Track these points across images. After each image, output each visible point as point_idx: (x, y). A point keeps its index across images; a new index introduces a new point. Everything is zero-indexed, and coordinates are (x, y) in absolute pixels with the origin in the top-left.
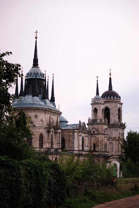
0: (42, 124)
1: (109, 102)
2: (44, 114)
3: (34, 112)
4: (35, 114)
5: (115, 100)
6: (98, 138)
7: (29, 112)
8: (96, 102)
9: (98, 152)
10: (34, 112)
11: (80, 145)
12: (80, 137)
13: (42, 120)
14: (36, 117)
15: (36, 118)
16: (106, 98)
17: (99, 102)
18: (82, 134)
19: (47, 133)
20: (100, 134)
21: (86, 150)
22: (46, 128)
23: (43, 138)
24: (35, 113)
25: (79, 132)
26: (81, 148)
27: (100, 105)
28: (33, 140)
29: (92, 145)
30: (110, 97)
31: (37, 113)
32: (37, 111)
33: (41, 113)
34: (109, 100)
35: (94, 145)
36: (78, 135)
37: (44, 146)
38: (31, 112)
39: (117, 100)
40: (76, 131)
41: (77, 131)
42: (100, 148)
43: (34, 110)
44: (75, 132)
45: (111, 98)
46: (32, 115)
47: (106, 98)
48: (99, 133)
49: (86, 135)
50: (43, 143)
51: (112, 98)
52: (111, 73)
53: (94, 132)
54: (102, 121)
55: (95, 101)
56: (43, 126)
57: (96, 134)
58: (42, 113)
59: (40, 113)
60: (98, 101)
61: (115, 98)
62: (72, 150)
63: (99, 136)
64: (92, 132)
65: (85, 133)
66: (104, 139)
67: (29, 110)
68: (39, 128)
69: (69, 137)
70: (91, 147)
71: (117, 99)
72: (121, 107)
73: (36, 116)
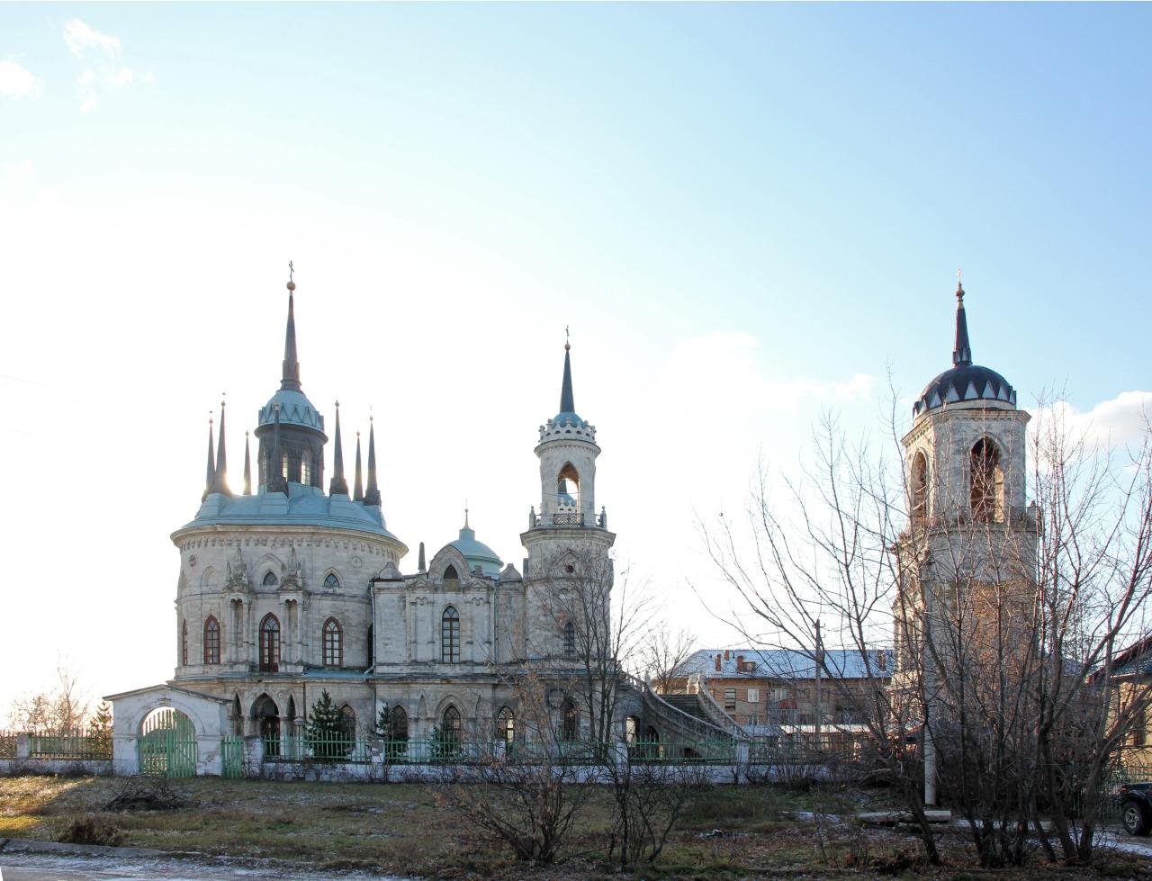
0: (216, 582)
10: (189, 548)
11: (424, 637)
15: (192, 566)
18: (430, 596)
19: (233, 612)
21: (478, 659)
23: (218, 631)
37: (223, 658)
40: (379, 589)
41: (395, 585)
49: (470, 596)
50: (219, 648)
58: (210, 544)
65: (465, 589)
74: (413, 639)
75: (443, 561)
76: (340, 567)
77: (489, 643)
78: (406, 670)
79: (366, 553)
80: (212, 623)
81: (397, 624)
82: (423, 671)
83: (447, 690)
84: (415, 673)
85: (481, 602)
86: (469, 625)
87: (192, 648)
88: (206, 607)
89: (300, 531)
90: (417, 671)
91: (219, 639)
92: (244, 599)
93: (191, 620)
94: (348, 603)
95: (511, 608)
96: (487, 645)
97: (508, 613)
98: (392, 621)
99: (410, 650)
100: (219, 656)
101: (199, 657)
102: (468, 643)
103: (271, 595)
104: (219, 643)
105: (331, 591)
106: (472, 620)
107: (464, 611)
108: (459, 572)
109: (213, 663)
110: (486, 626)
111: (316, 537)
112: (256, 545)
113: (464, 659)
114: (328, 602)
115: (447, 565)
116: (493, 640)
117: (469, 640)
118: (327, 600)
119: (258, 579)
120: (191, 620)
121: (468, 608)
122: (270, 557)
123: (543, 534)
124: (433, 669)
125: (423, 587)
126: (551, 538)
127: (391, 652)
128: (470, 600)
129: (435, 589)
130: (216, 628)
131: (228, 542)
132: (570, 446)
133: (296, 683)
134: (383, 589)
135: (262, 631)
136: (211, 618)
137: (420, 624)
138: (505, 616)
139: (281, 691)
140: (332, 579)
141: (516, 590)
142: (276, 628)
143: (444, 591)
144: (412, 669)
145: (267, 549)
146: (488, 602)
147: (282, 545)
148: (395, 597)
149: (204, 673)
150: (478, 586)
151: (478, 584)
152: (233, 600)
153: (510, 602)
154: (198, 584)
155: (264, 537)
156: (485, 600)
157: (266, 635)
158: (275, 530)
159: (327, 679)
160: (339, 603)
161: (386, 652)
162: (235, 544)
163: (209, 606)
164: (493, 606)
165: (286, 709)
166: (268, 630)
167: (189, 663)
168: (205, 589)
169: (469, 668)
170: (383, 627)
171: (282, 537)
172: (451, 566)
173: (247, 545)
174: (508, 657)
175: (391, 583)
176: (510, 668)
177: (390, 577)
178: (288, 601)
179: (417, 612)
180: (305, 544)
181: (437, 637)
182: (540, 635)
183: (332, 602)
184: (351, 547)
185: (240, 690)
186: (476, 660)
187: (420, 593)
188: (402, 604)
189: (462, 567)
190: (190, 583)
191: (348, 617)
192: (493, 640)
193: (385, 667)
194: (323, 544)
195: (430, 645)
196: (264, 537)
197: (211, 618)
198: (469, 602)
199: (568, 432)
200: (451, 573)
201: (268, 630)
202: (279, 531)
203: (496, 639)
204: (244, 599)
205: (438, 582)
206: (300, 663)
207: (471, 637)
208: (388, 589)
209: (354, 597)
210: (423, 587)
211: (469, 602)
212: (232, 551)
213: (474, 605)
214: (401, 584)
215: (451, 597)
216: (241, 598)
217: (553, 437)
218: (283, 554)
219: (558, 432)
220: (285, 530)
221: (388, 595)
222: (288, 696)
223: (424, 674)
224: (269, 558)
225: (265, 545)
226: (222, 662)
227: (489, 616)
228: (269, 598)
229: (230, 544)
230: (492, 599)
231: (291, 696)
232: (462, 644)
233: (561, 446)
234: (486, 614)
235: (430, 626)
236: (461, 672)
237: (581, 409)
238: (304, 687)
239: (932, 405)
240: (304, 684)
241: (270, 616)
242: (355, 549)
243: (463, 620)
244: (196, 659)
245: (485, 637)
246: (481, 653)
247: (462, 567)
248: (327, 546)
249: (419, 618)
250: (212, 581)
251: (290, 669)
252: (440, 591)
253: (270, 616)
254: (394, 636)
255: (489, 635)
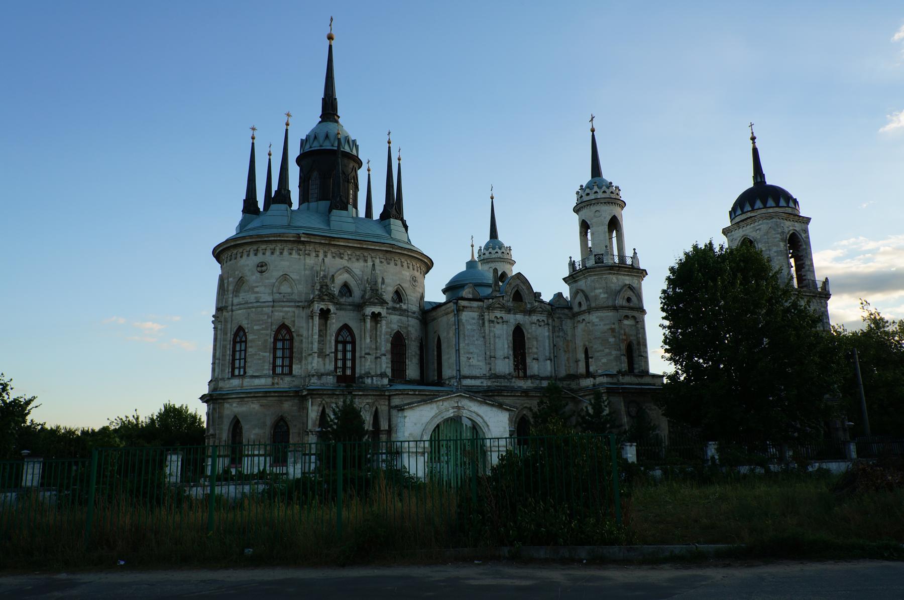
0: (289, 290)
1: (749, 221)
2: (295, 255)
3: (256, 255)
4: (260, 258)
5: (771, 210)
6: (594, 324)
7: (241, 257)
8: (585, 198)
9: (594, 377)
10: (256, 255)
11: (500, 353)
12: (498, 326)
13: (285, 277)
14: (259, 269)
15: (261, 272)
16: (739, 212)
17: (592, 197)
18: (506, 316)
19: (310, 321)
20: (598, 309)
22: (306, 304)
23: (291, 340)
24: (260, 254)
25: (490, 308)
26: (504, 366)
27: (597, 208)
28: (250, 351)
29: (581, 356)
30: (752, 206)
31: (264, 254)
32: (264, 247)
33: (281, 253)
34: (749, 215)
35: (586, 352)
36: (483, 319)
37: (296, 369)
38: (245, 257)
39: (777, 209)
40: (464, 307)
41: (475, 304)
42: (604, 360)
43: (255, 247)
44: (459, 310)
45: (756, 207)
46: (248, 265)
47: (739, 212)
48: (593, 305)
49: (534, 318)
50: (291, 358)
51: (759, 204)
52: (755, 135)
53: (580, 304)
54: (603, 262)
55: (582, 197)
56: (296, 297)
57: (584, 312)
58: (286, 253)
59: (277, 252)
60: (588, 194)
61: (771, 203)
62: (453, 378)
63: (594, 317)
64: (576, 309)
65: (530, 312)
66: (616, 326)
67: (241, 250)
68: (273, 307)
69: (448, 333)
70: (577, 361)
71: (778, 206)
72: (806, 231)
73: (262, 266)
74: (492, 354)
75: (513, 286)
76: (403, 285)
77: (551, 360)
78: (486, 383)
79: (419, 273)
80: (284, 332)
81: (477, 340)
82: (503, 384)
83: (523, 402)
84: (496, 386)
85: (543, 324)
86: (535, 343)
87: (258, 357)
88: (278, 315)
89: (377, 248)
90: (498, 384)
91: (291, 349)
92: (332, 308)
93: (255, 328)
94: (410, 319)
95: (563, 330)
96: (549, 362)
97: (561, 334)
98: (473, 336)
99: (490, 364)
100: (291, 367)
101: (267, 367)
102: (534, 359)
103: (349, 307)
104: (292, 352)
105: (398, 306)
106: (537, 340)
107: (530, 331)
108: (523, 299)
109: (283, 374)
110: (547, 344)
111: (388, 256)
112: (334, 257)
113: (532, 374)
114: (395, 317)
115: (516, 289)
116: (552, 358)
117: (536, 356)
118: (395, 314)
119: (336, 289)
120: (255, 328)
121: (533, 327)
122: (348, 270)
123: (610, 270)
124: (511, 382)
125: (500, 308)
126: (614, 274)
127: (473, 365)
128: (535, 321)
129: (509, 311)
130: (287, 337)
131: (307, 252)
132: (612, 203)
133: (385, 395)
134: (467, 307)
135: (337, 342)
136: (283, 326)
137: (497, 340)
138: (558, 337)
139: (368, 403)
140: (399, 295)
141: (564, 314)
142: (349, 339)
143: (515, 314)
144: (493, 382)
145: (344, 262)
146: (548, 324)
147: (358, 260)
148: (475, 315)
149: (273, 384)
150: (540, 309)
151: (541, 307)
152: (322, 310)
153: (561, 325)
154: (271, 292)
155: (342, 251)
156: (546, 322)
157: (340, 347)
158: (356, 245)
159: (420, 391)
160: (404, 319)
161: (470, 366)
162: (314, 254)
163: (281, 314)
164: (551, 328)
165: (371, 422)
166: (346, 337)
167: (250, 372)
168: (277, 296)
169: (538, 382)
170: (466, 342)
171: (358, 253)
172: (517, 290)
173: (326, 256)
174: (563, 373)
175: (472, 302)
176: (565, 383)
177: (470, 296)
178: (373, 313)
179: (495, 329)
180: (377, 261)
181: (511, 352)
182: (610, 354)
183: (399, 317)
184: (411, 267)
185: (327, 403)
186: (541, 375)
187: (498, 314)
188: (481, 322)
189: (527, 292)
190: (256, 290)
191: (410, 331)
192: (552, 358)
193: (469, 380)
194: (392, 263)
195: (507, 360)
196: (342, 251)
197: (283, 326)
198: (534, 323)
199: (612, 192)
200: (518, 297)
201: (346, 337)
202: (359, 246)
203: (555, 357)
204: (332, 308)
205: (510, 304)
206: (383, 375)
207: (536, 353)
208: (471, 307)
209: (414, 313)
210: (500, 308)
211: (534, 323)
212: (310, 261)
213: (537, 326)
214: (480, 303)
215: (520, 318)
216: (329, 308)
217: (600, 195)
218: (358, 267)
219: (604, 192)
220: (364, 246)
221: (471, 313)
222: (374, 409)
223: (504, 386)
224: (347, 272)
225: (342, 258)
226: (294, 372)
227: (549, 336)
228: (345, 310)
229: (309, 255)
230: (550, 321)
231: (377, 407)
232: (528, 360)
233: (609, 203)
234: (547, 334)
235: (506, 342)
236: (532, 385)
237: (607, 174)
238: (389, 400)
239: (745, 210)
240: (389, 396)
241: (346, 327)
242: (414, 269)
243: (528, 338)
244: (263, 370)
245: (547, 354)
246: (546, 368)
247: (527, 292)
248: (396, 265)
249: (496, 335)
250: (285, 288)
251: (377, 382)
252: (512, 312)
253: (346, 327)
254: (475, 350)
255: (550, 353)
